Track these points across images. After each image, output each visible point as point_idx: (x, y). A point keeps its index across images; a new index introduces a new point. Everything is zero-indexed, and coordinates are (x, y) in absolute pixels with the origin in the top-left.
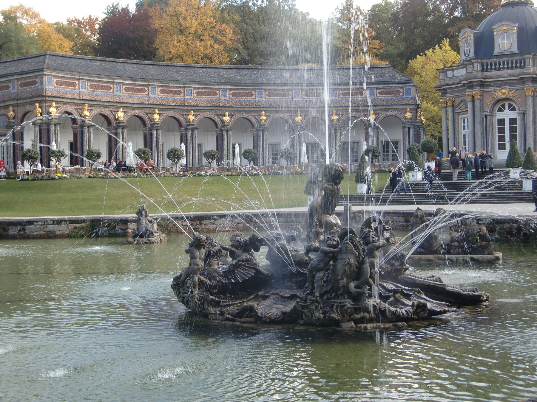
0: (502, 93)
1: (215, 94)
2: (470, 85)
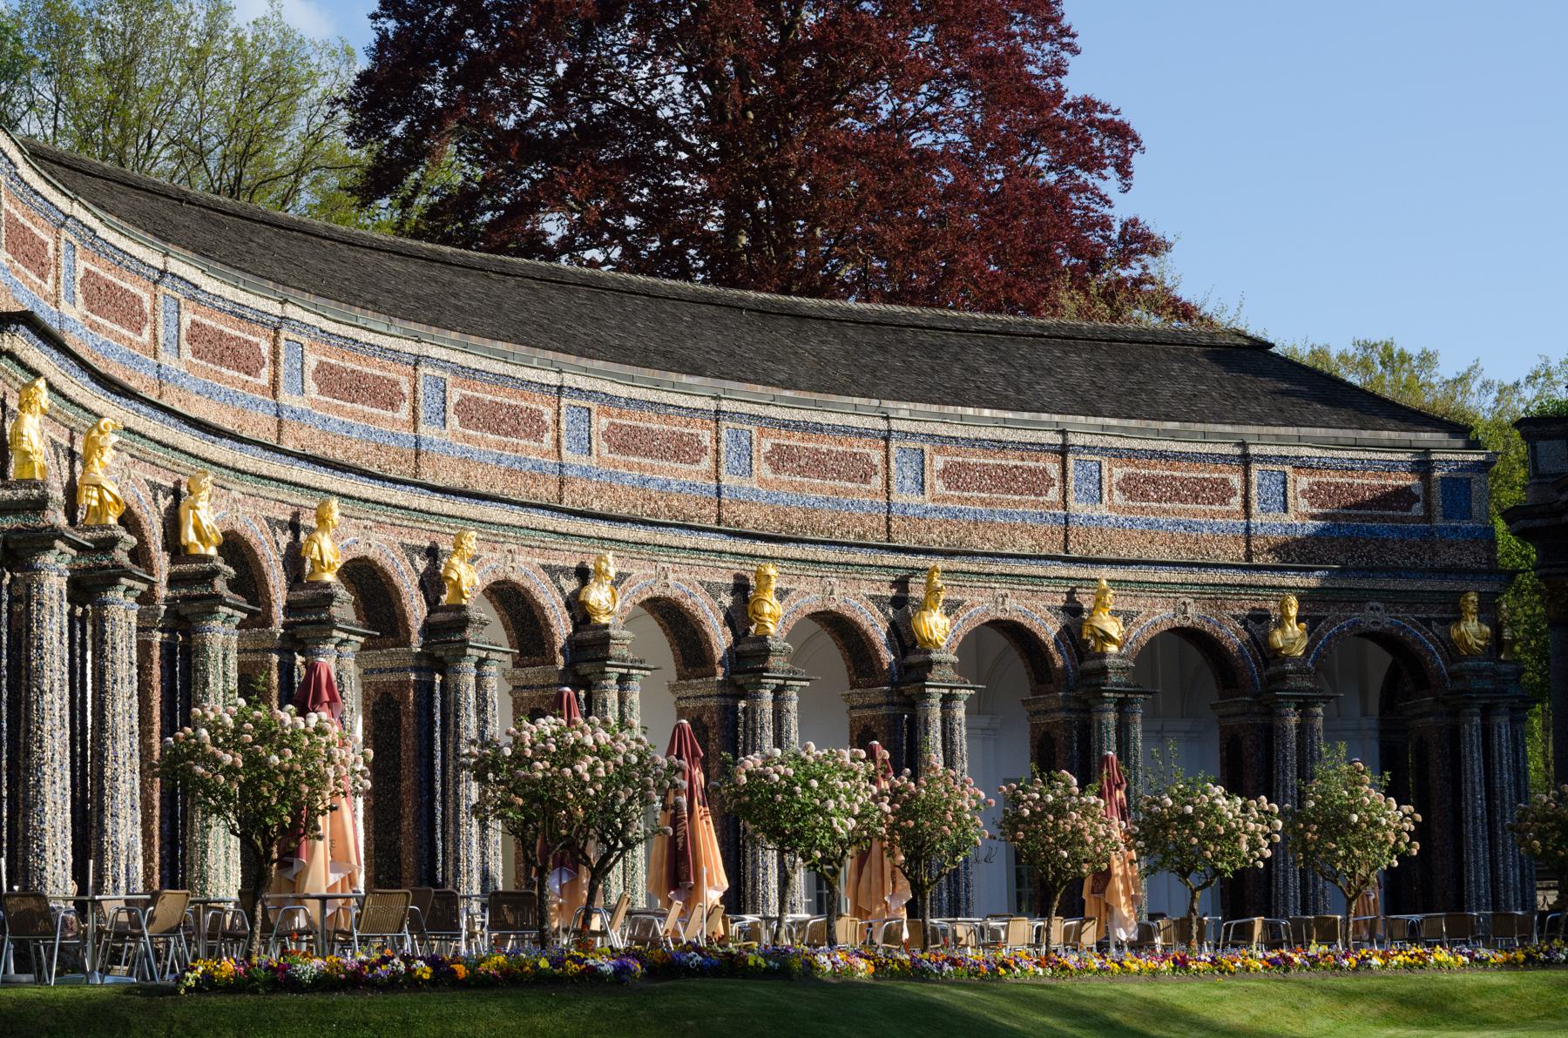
1: (529, 424)
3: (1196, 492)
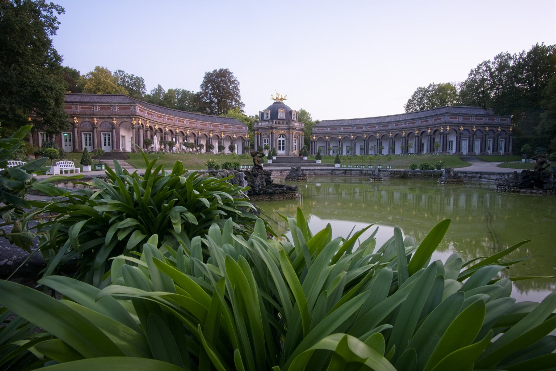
0: (283, 132)
1: (183, 122)
2: (272, 129)
3: (229, 127)
